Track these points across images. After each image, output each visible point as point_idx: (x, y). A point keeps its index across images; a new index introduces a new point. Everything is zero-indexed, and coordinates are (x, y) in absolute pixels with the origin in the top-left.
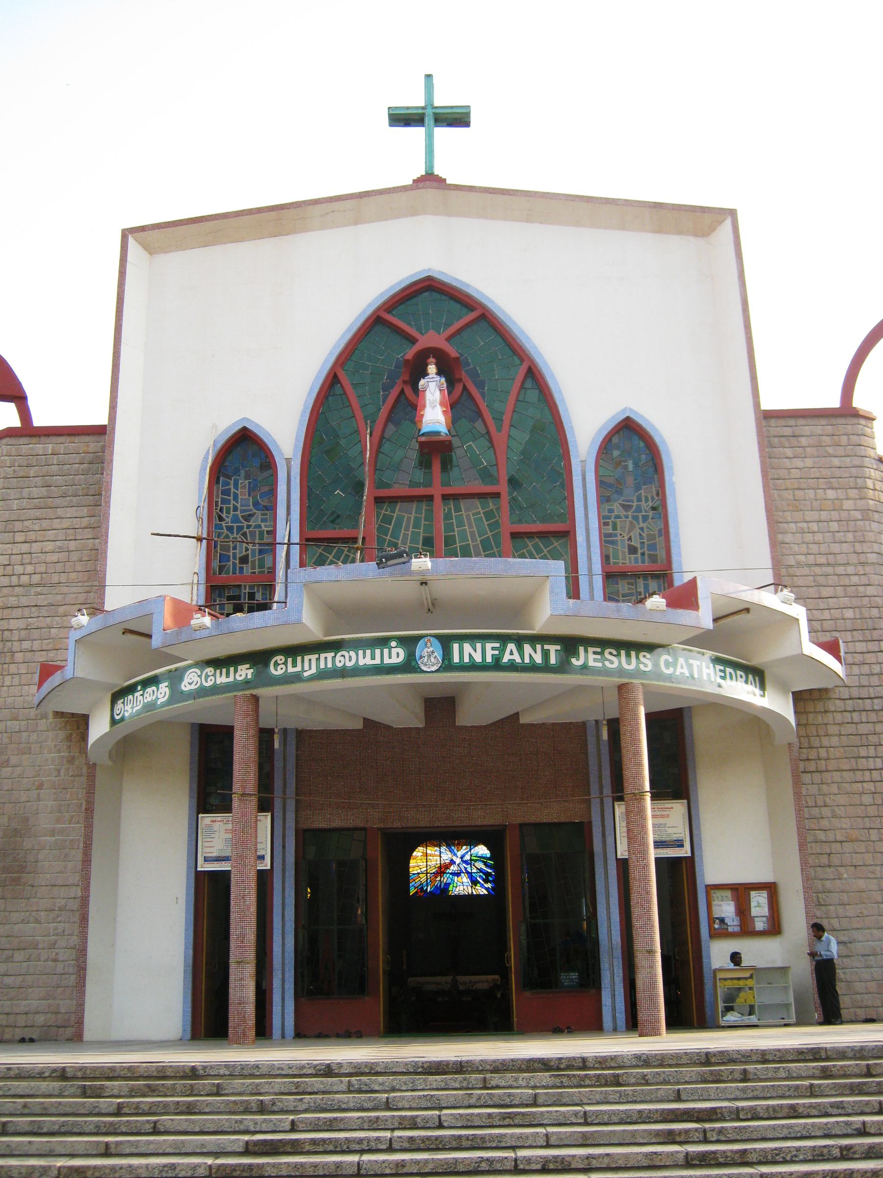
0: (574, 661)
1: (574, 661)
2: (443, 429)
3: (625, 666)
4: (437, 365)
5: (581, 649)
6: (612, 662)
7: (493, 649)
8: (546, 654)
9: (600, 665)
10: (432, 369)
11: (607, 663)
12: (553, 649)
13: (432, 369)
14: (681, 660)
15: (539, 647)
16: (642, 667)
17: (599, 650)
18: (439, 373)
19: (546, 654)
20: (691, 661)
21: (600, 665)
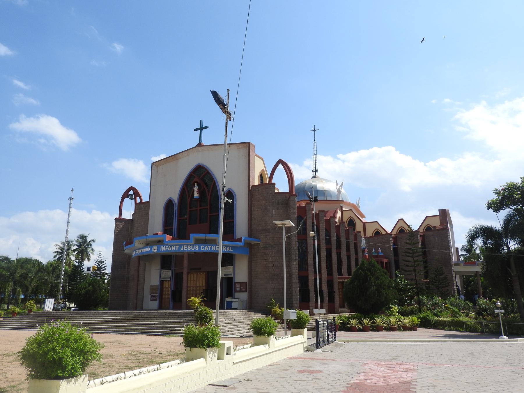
0: (181, 249)
1: (181, 249)
2: (194, 198)
3: (192, 249)
4: (197, 184)
5: (183, 246)
6: (189, 249)
7: (167, 247)
8: (176, 248)
9: (186, 249)
10: (196, 185)
11: (188, 249)
12: (177, 246)
13: (196, 185)
14: (206, 246)
15: (174, 246)
16: (196, 249)
17: (187, 246)
18: (197, 186)
19: (176, 248)
20: (209, 246)
21: (186, 249)
